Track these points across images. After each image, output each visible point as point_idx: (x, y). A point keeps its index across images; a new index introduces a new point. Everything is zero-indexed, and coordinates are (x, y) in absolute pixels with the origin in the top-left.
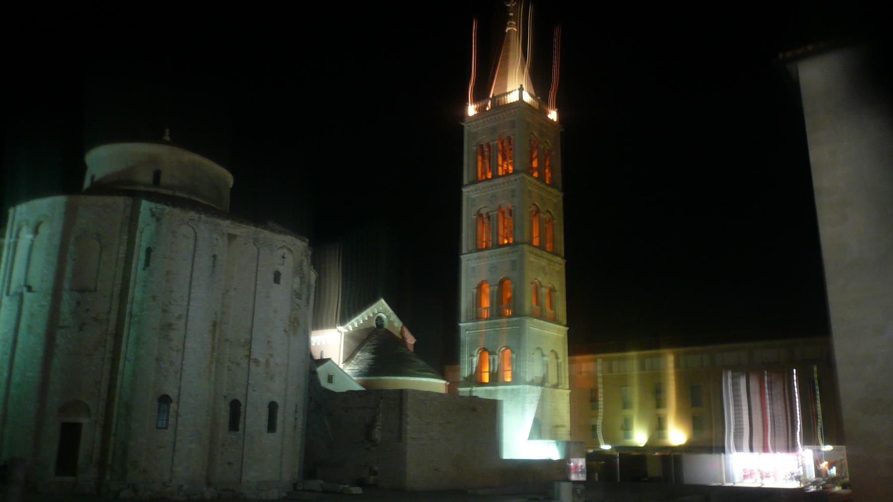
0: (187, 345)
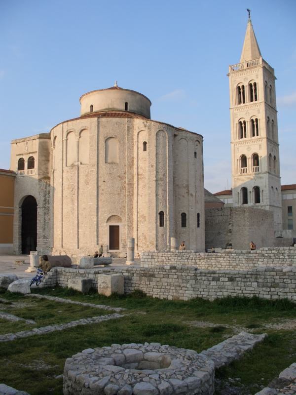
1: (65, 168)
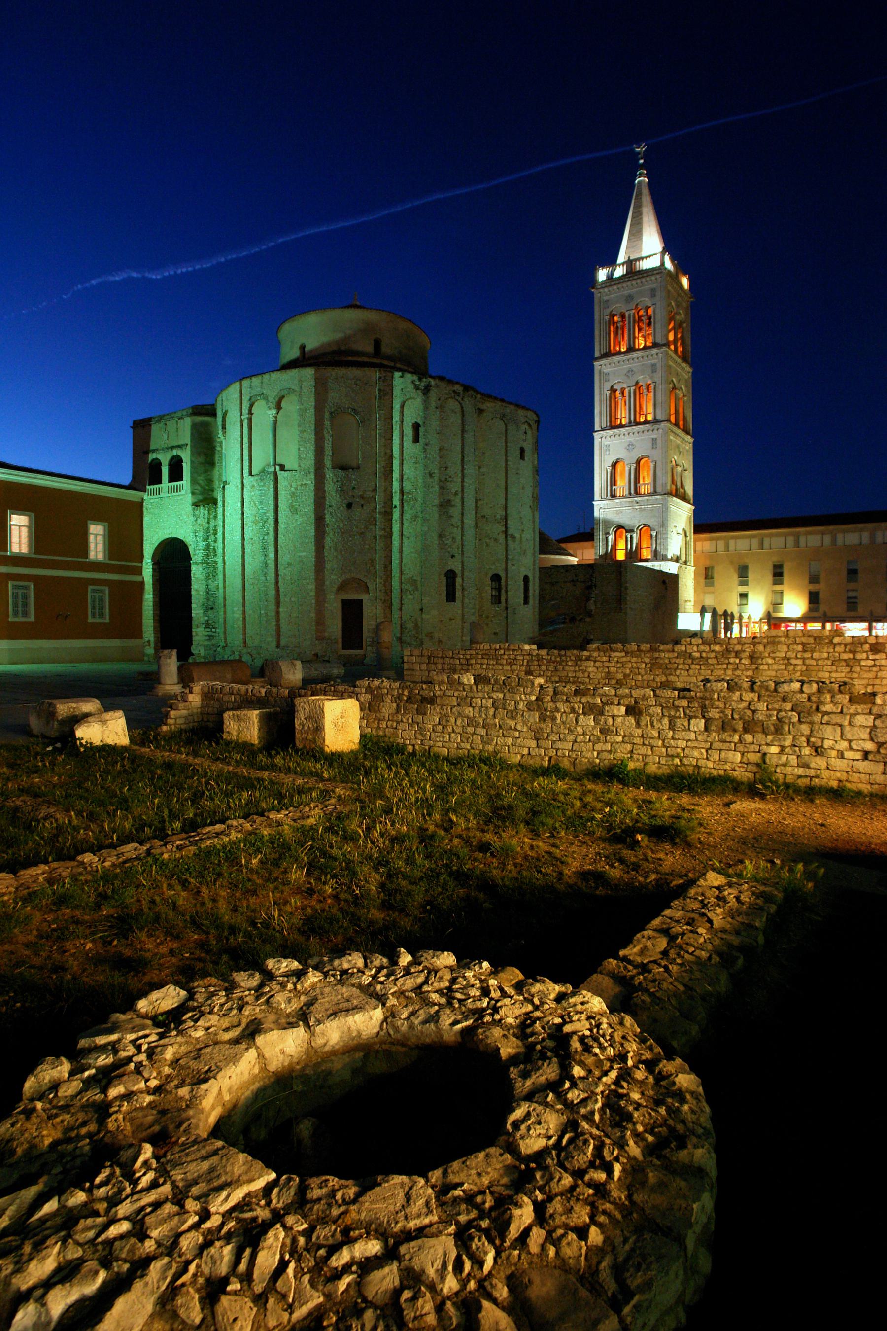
0: (465, 521)
1: (248, 480)
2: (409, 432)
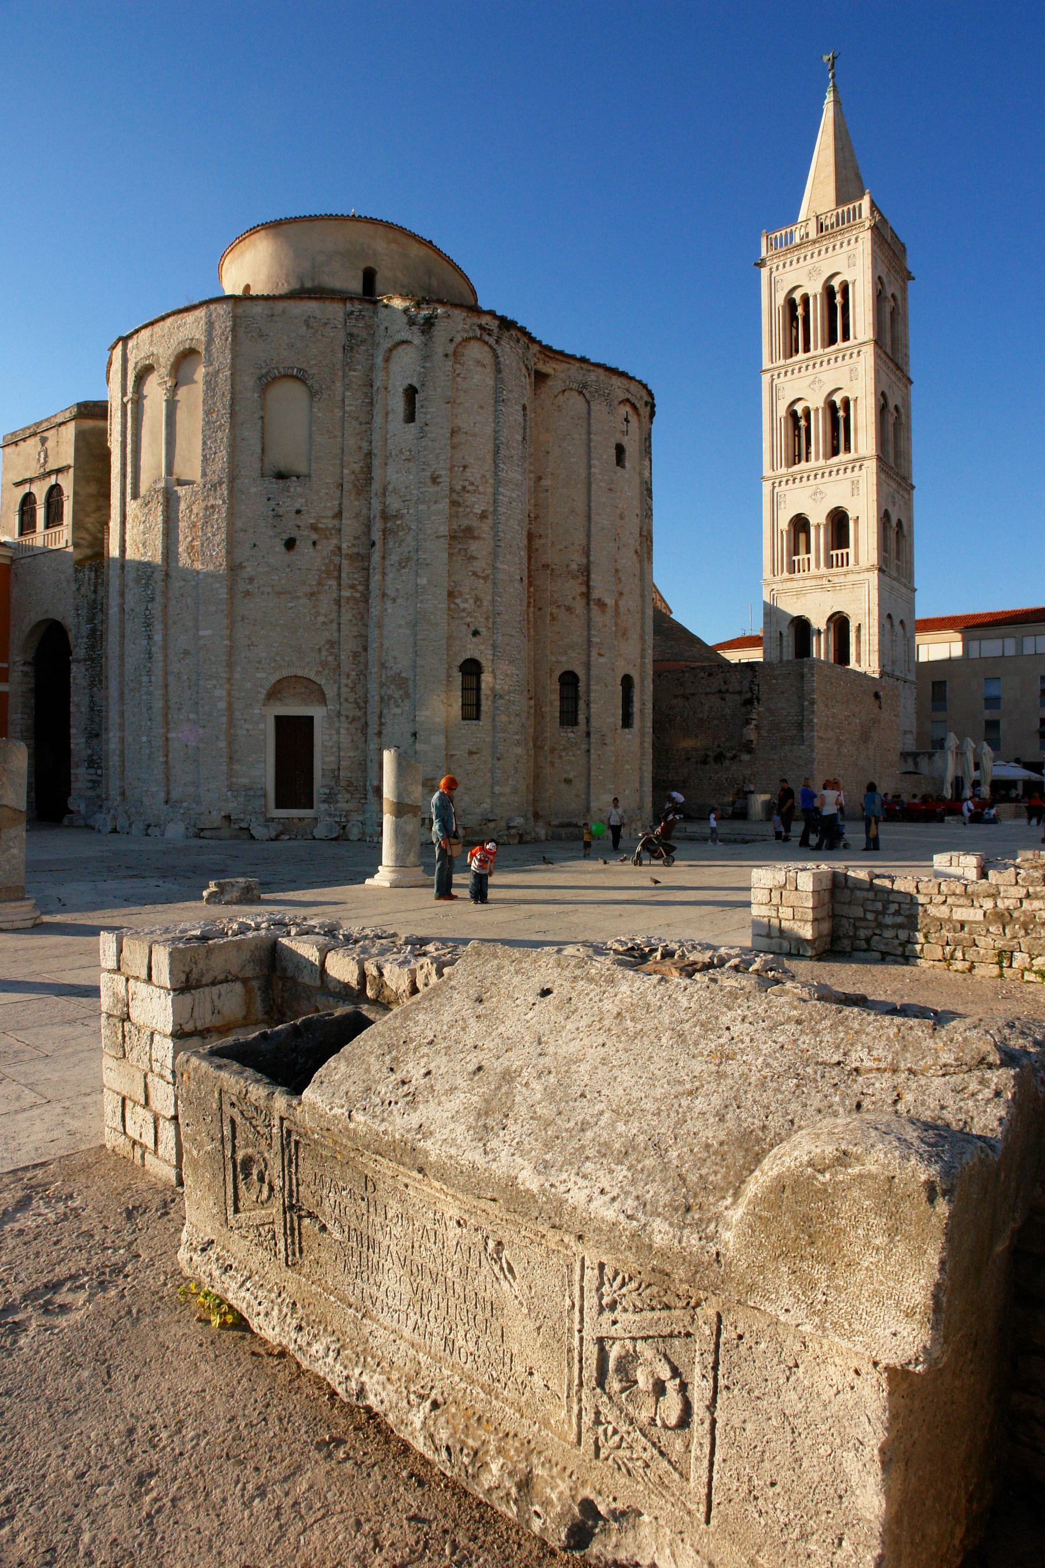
1: (132, 506)
2: (398, 404)
